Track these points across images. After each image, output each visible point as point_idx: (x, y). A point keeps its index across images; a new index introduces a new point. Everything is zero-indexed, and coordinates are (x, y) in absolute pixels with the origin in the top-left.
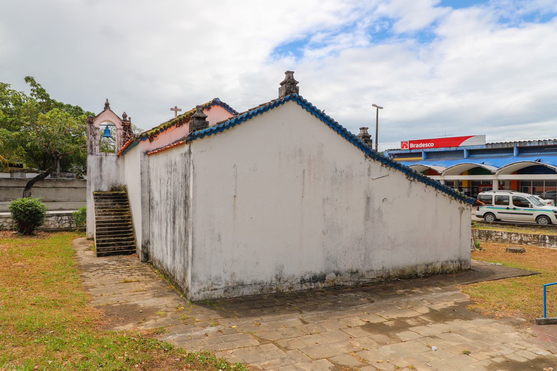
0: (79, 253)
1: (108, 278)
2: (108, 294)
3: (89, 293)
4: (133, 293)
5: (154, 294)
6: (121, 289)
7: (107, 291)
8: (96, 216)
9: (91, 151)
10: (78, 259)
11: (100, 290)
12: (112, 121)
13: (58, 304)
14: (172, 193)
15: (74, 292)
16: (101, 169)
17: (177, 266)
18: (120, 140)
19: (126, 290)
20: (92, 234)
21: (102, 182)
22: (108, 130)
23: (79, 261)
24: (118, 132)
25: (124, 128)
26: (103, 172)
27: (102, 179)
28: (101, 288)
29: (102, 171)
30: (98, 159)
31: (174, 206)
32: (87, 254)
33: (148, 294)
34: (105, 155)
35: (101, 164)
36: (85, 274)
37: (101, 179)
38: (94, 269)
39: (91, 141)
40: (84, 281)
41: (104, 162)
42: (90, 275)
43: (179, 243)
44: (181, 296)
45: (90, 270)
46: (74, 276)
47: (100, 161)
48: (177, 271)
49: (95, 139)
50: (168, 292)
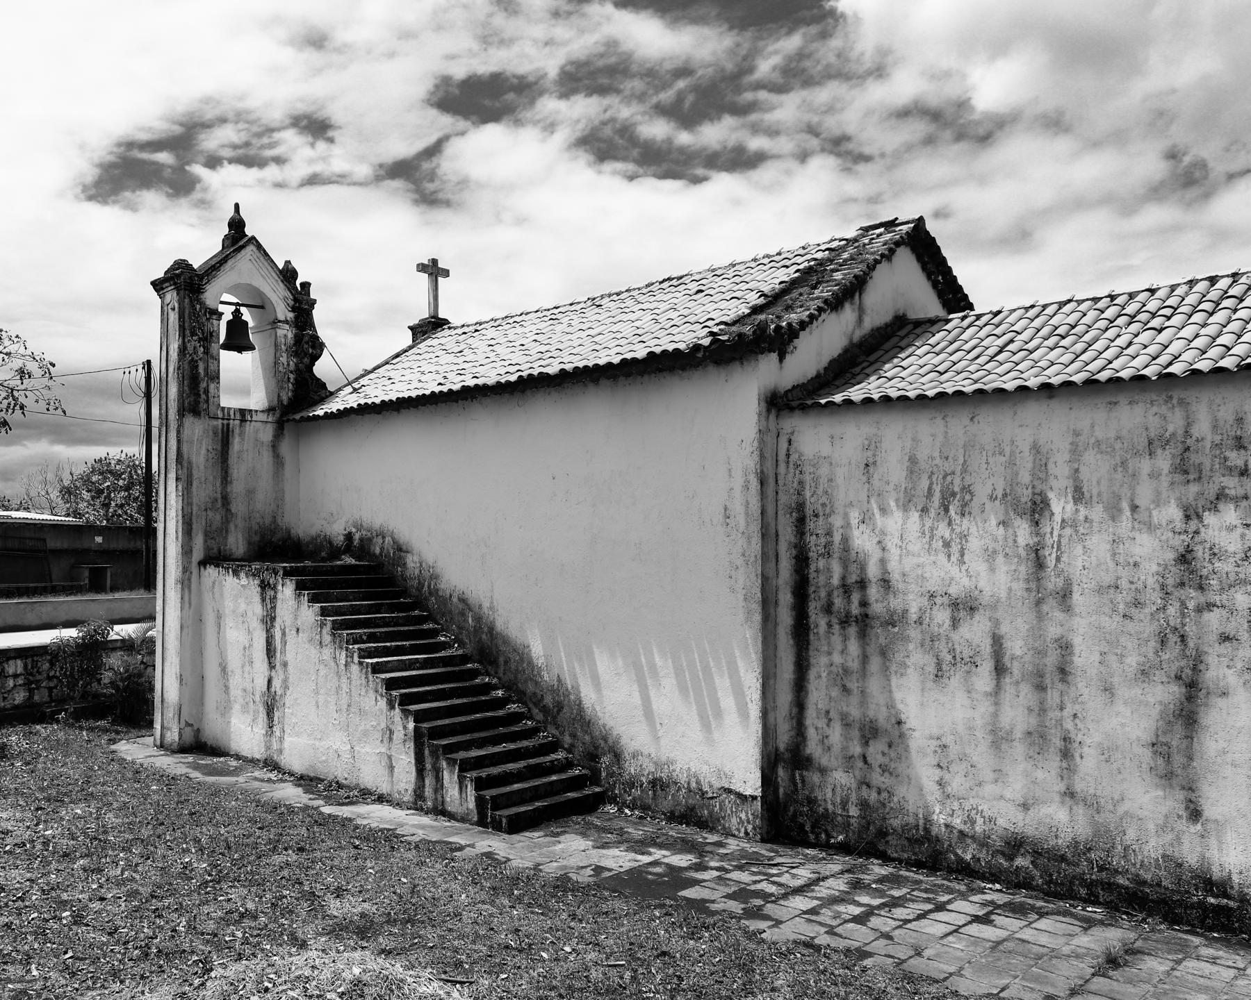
16: (226, 472)
27: (228, 510)
30: (215, 433)
34: (238, 417)
35: (227, 452)
47: (222, 441)
49: (207, 352)
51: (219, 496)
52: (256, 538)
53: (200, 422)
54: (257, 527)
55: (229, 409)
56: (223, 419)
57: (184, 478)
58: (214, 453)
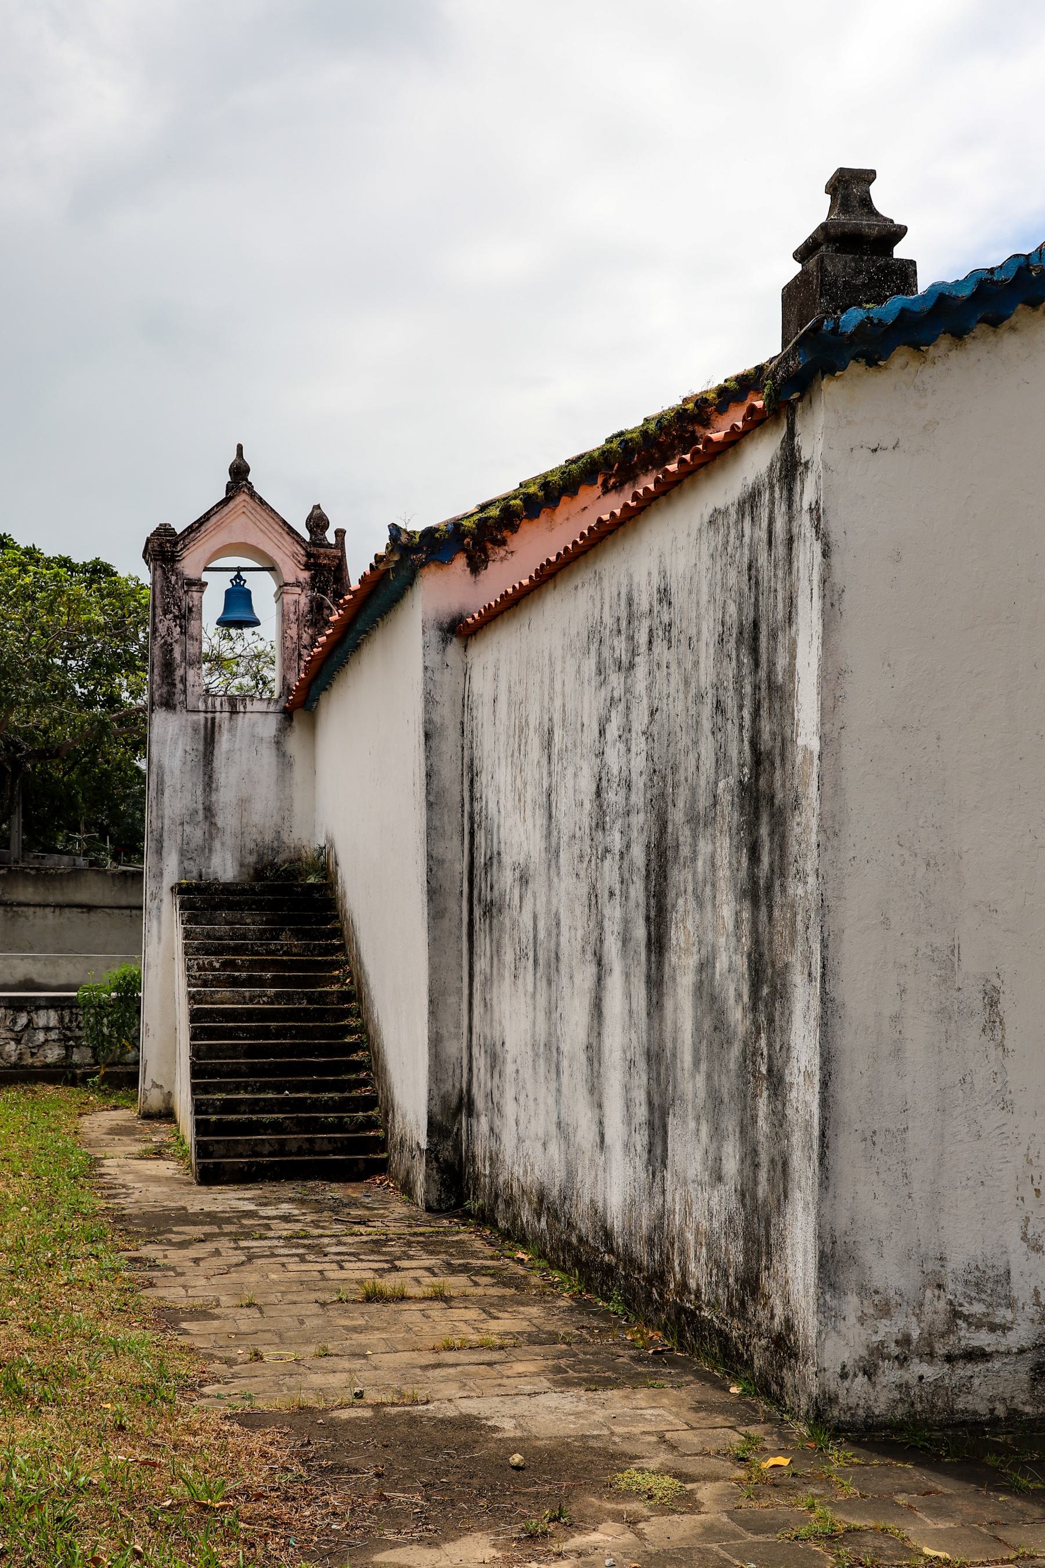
0: (110, 1167)
1: (273, 1276)
2: (290, 1354)
3: (184, 1341)
4: (430, 1358)
5: (558, 1370)
6: (355, 1329)
7: (281, 1338)
8: (189, 986)
10: (110, 1191)
11: (243, 1328)
13: (23, 1382)
14: (634, 776)
15: (108, 1328)
17: (688, 1205)
19: (384, 1336)
20: (166, 1091)
21: (212, 838)
22: (240, 592)
23: (115, 1196)
28: (246, 1321)
30: (195, 730)
31: (658, 846)
32: (148, 1172)
33: (519, 1368)
34: (226, 707)
36: (148, 1251)
37: (206, 827)
38: (197, 1231)
40: (152, 1285)
41: (224, 743)
42: (175, 1256)
43: (696, 1062)
44: (734, 1390)
45: (175, 1238)
46: (97, 1257)
48: (690, 1237)
49: (184, 632)
50: (638, 1360)
52: (252, 859)
53: (175, 717)
54: (253, 846)
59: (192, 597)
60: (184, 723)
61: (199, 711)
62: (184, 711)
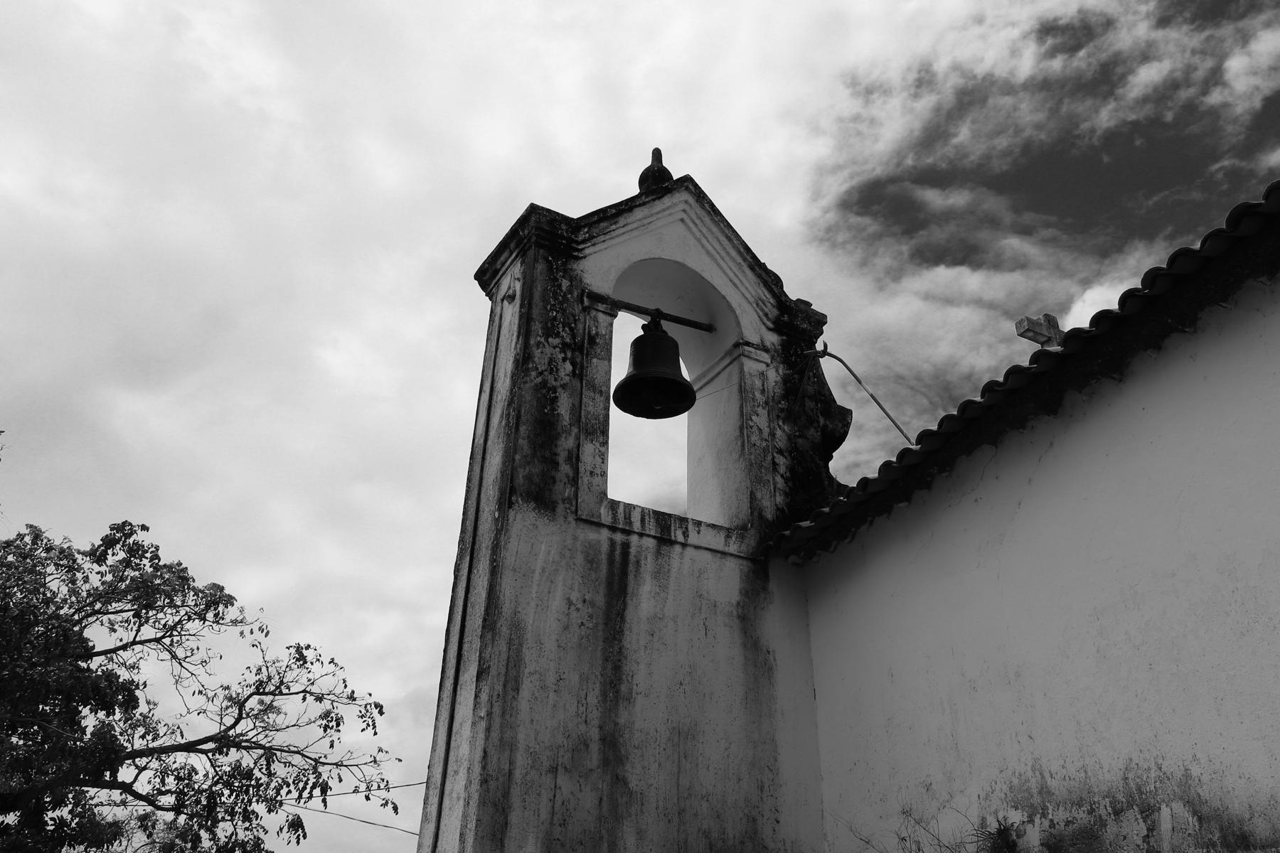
9: (536, 469)
12: (706, 275)
16: (617, 668)
18: (766, 435)
24: (750, 366)
25: (783, 344)
26: (629, 699)
27: (619, 781)
29: (624, 688)
30: (591, 562)
35: (621, 614)
39: (544, 384)
47: (610, 584)
49: (579, 373)
51: (595, 734)
55: (629, 508)
56: (613, 529)
57: (497, 667)
58: (586, 611)
59: (595, 319)
60: (569, 542)
61: (599, 525)
62: (571, 518)
